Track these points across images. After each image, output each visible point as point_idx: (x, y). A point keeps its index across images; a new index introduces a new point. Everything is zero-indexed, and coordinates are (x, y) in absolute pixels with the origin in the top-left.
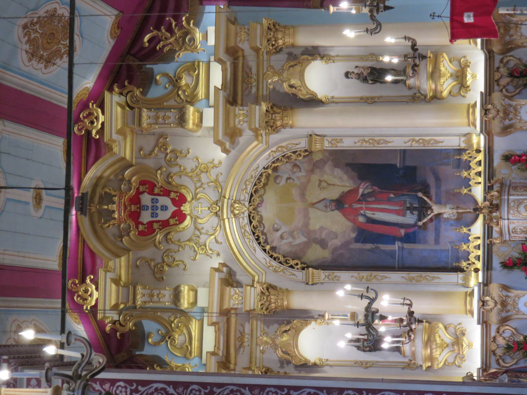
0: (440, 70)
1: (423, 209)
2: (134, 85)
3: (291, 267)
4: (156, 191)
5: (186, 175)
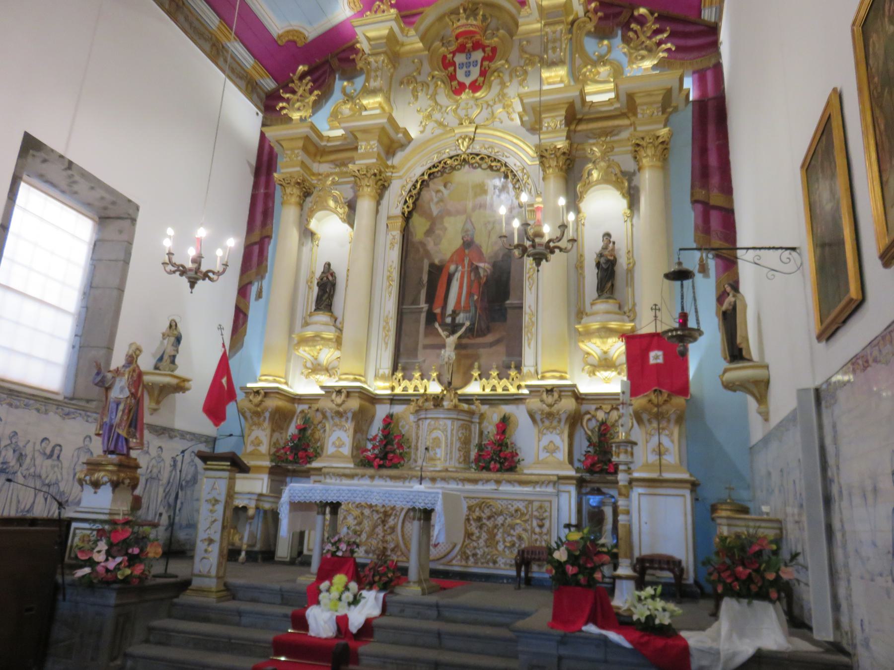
0: (607, 338)
1: (453, 328)
2: (598, 24)
3: (406, 202)
4: (486, 63)
5: (502, 89)
